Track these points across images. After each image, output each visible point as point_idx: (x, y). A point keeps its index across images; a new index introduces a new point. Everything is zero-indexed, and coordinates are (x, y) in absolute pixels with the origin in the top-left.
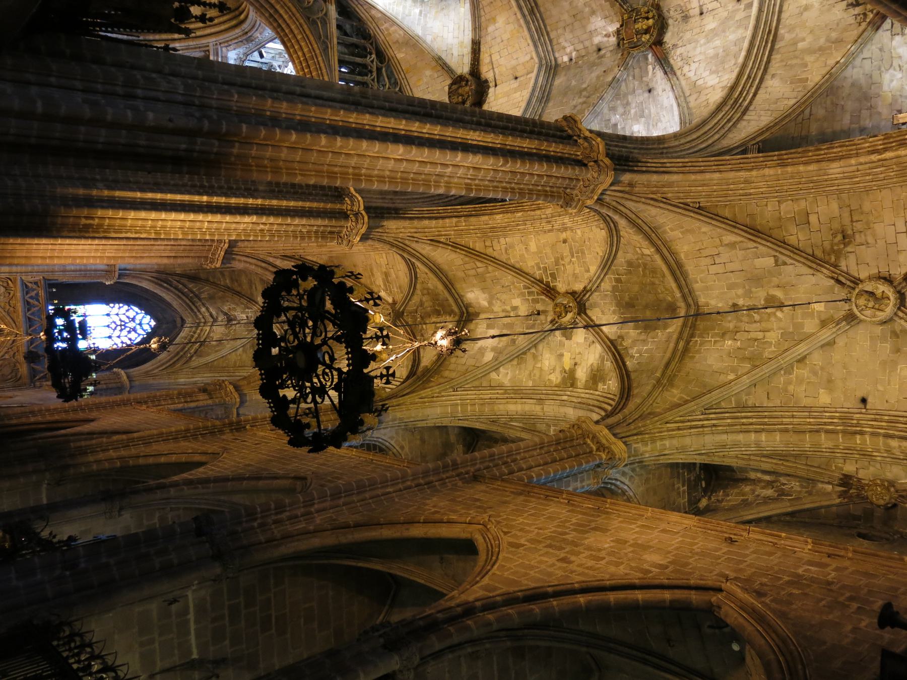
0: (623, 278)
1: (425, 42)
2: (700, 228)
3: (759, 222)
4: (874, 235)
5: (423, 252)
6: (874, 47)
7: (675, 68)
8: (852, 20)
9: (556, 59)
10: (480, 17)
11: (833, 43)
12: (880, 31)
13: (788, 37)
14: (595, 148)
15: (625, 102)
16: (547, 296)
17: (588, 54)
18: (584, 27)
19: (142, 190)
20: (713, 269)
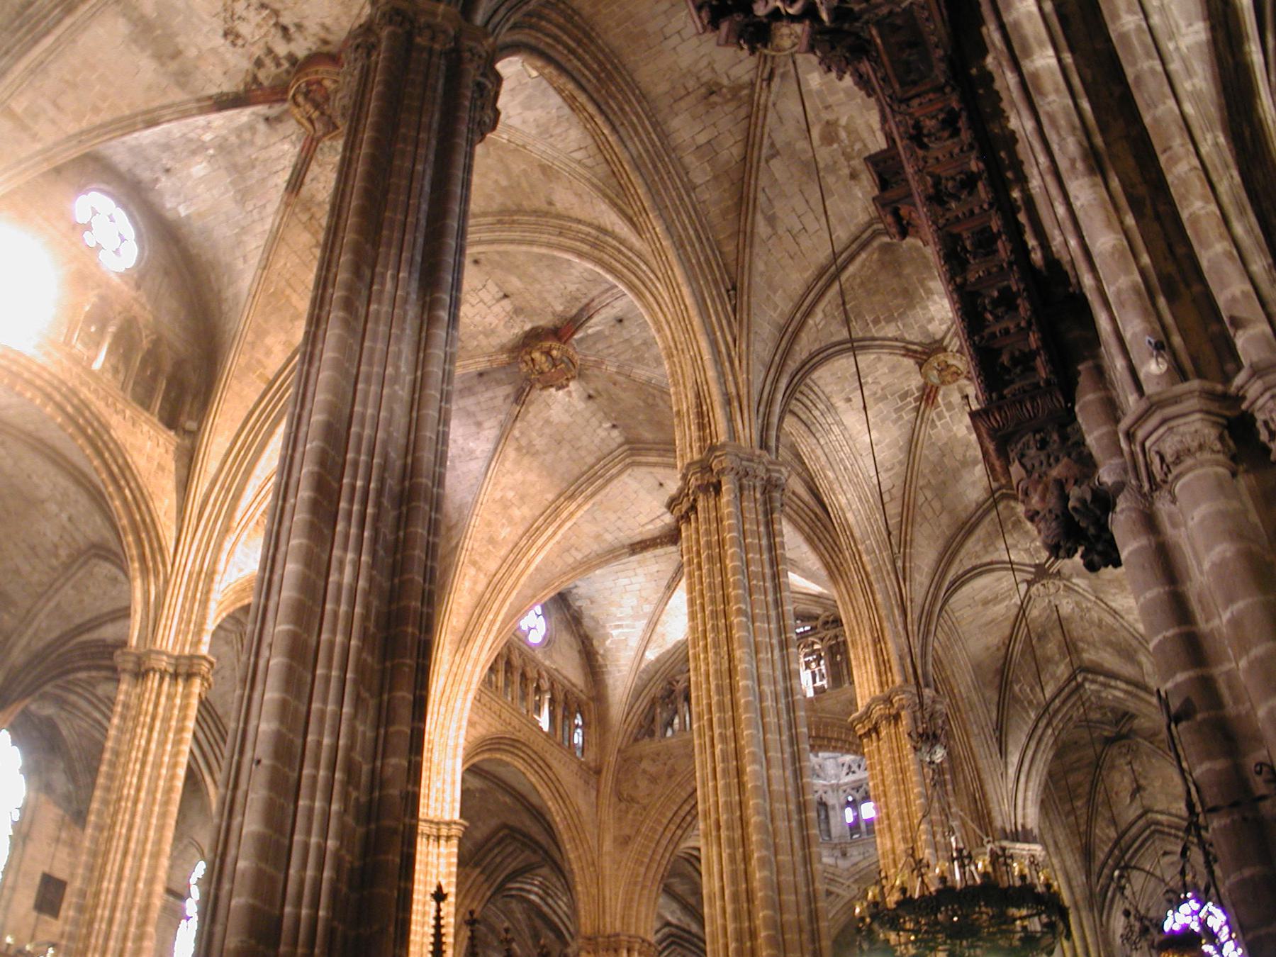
0: (869, 318)
2: (762, 274)
4: (696, 62)
5: (926, 582)
9: (620, 446)
13: (499, 199)
15: (644, 348)
16: (935, 397)
18: (568, 426)
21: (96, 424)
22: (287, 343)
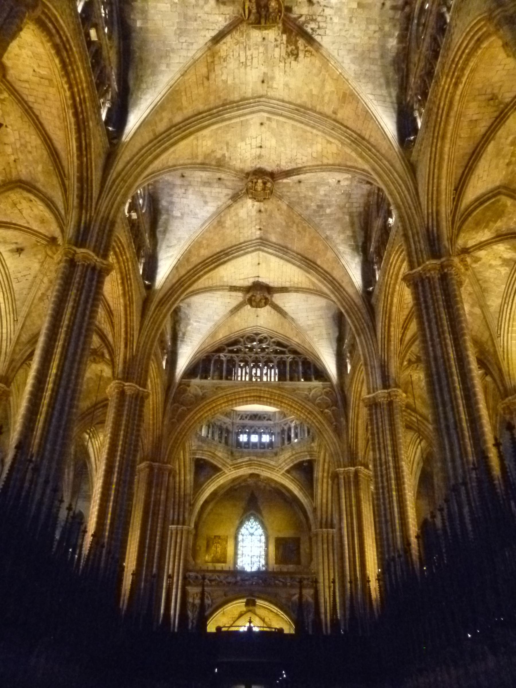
3: (469, 151)
7: (295, 166)
9: (257, 239)
10: (216, 286)
12: (323, 43)
18: (244, 220)
20: (485, 178)
22: (170, 120)
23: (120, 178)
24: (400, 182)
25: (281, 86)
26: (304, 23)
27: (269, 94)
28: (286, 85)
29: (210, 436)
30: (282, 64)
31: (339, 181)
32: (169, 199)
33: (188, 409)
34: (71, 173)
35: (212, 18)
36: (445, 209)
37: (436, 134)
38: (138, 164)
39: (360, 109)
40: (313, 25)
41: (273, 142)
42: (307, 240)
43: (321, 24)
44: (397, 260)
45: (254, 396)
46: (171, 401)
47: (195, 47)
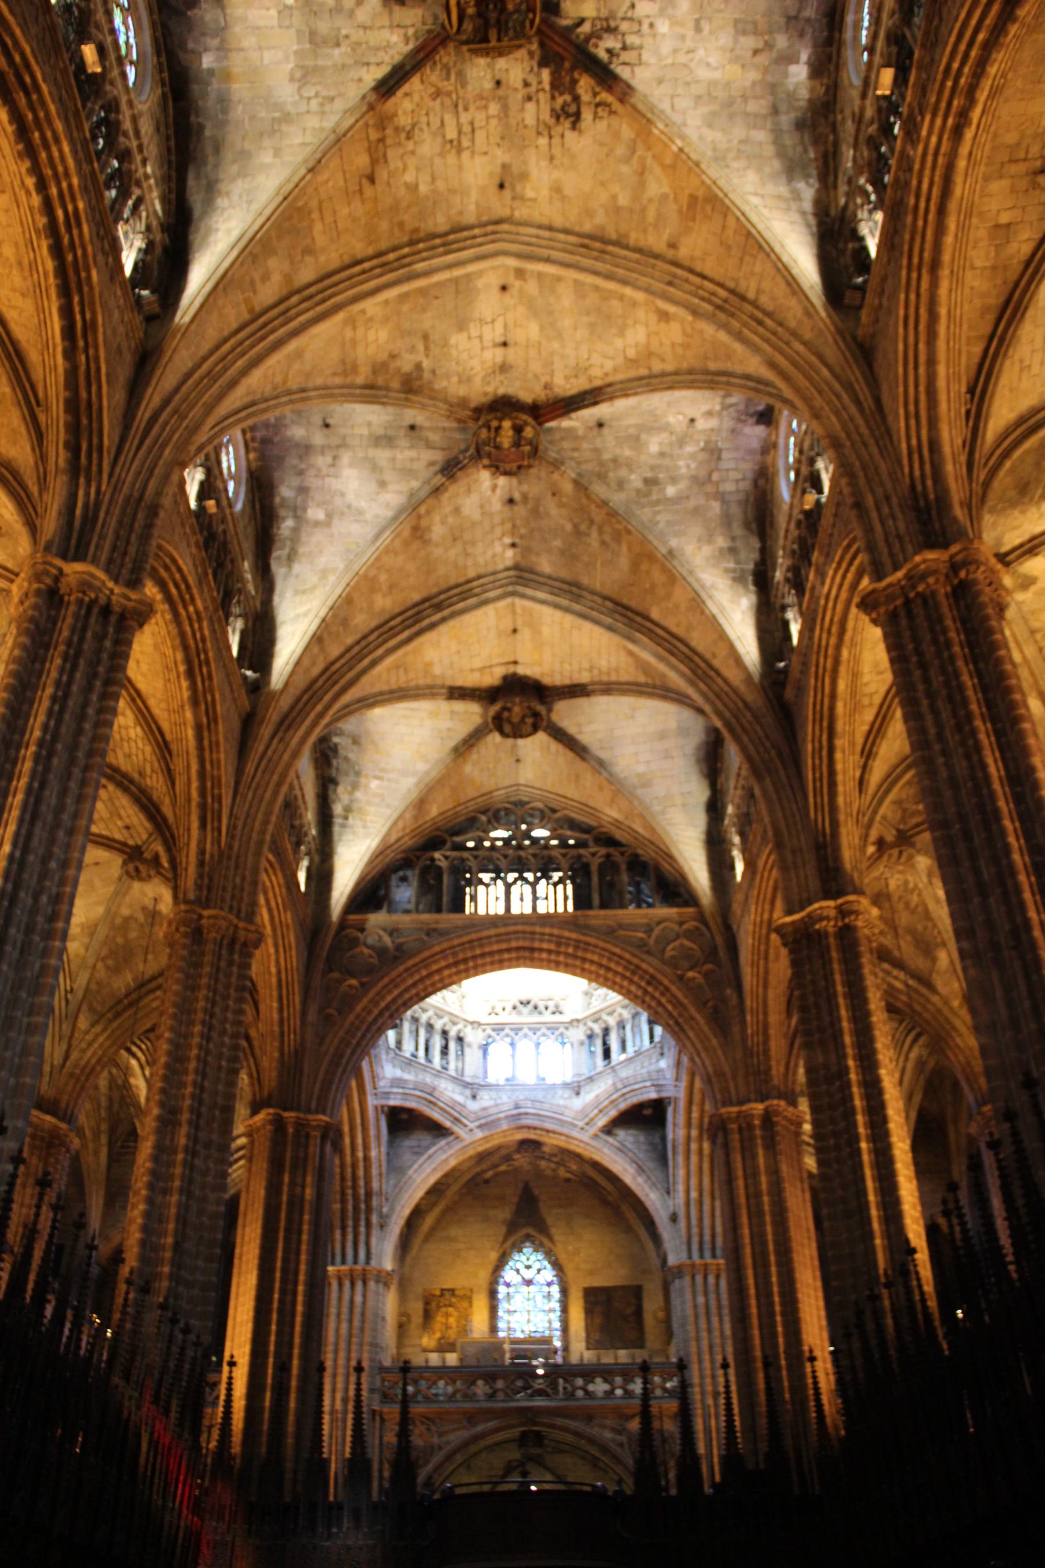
1: (427, 773)
3: (995, 300)
6: (656, 93)
8: (602, 125)
9: (507, 569)
10: (417, 688)
11: (634, 152)
12: (634, 83)
13: (600, 219)
14: (933, 566)
15: (611, 465)
17: (512, 519)
18: (474, 524)
19: (871, 1236)
20: (1036, 369)
21: (79, 253)
22: (288, 278)
23: (169, 409)
24: (837, 387)
25: (545, 192)
26: (588, 38)
27: (517, 214)
28: (557, 189)
29: (421, 1052)
30: (543, 141)
31: (692, 420)
32: (295, 481)
33: (362, 984)
34: (52, 393)
35: (376, 38)
36: (951, 435)
37: (916, 260)
38: (212, 377)
39: (730, 232)
40: (610, 42)
41: (533, 330)
42: (624, 561)
43: (630, 40)
44: (841, 586)
45: (518, 949)
46: (321, 965)
47: (339, 105)
